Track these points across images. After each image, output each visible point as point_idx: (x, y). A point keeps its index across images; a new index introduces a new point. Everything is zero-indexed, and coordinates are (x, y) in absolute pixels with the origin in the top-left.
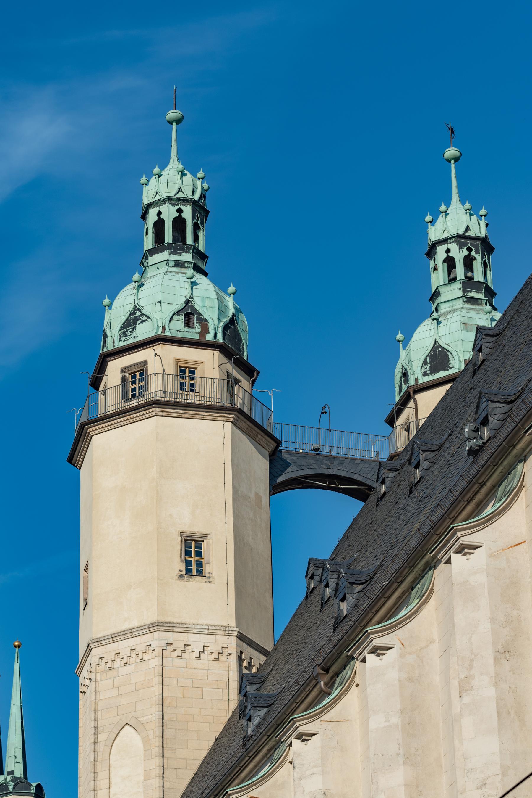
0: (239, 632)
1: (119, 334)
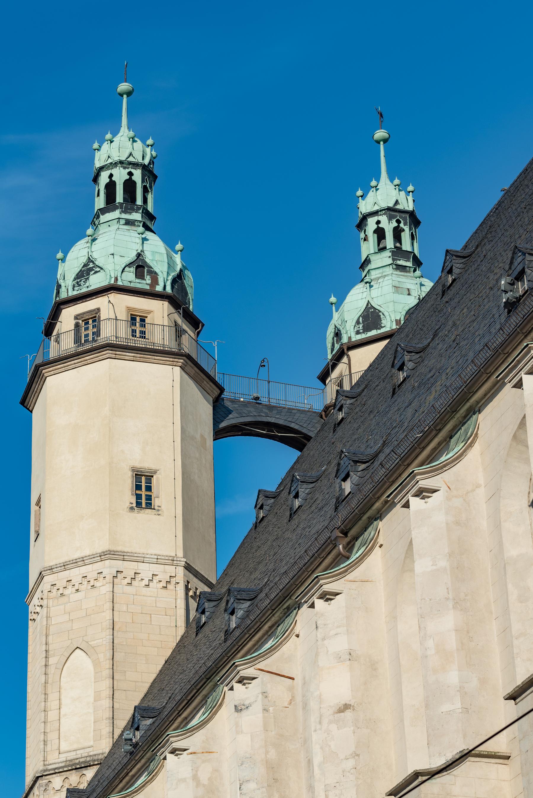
0: (186, 562)
1: (73, 284)
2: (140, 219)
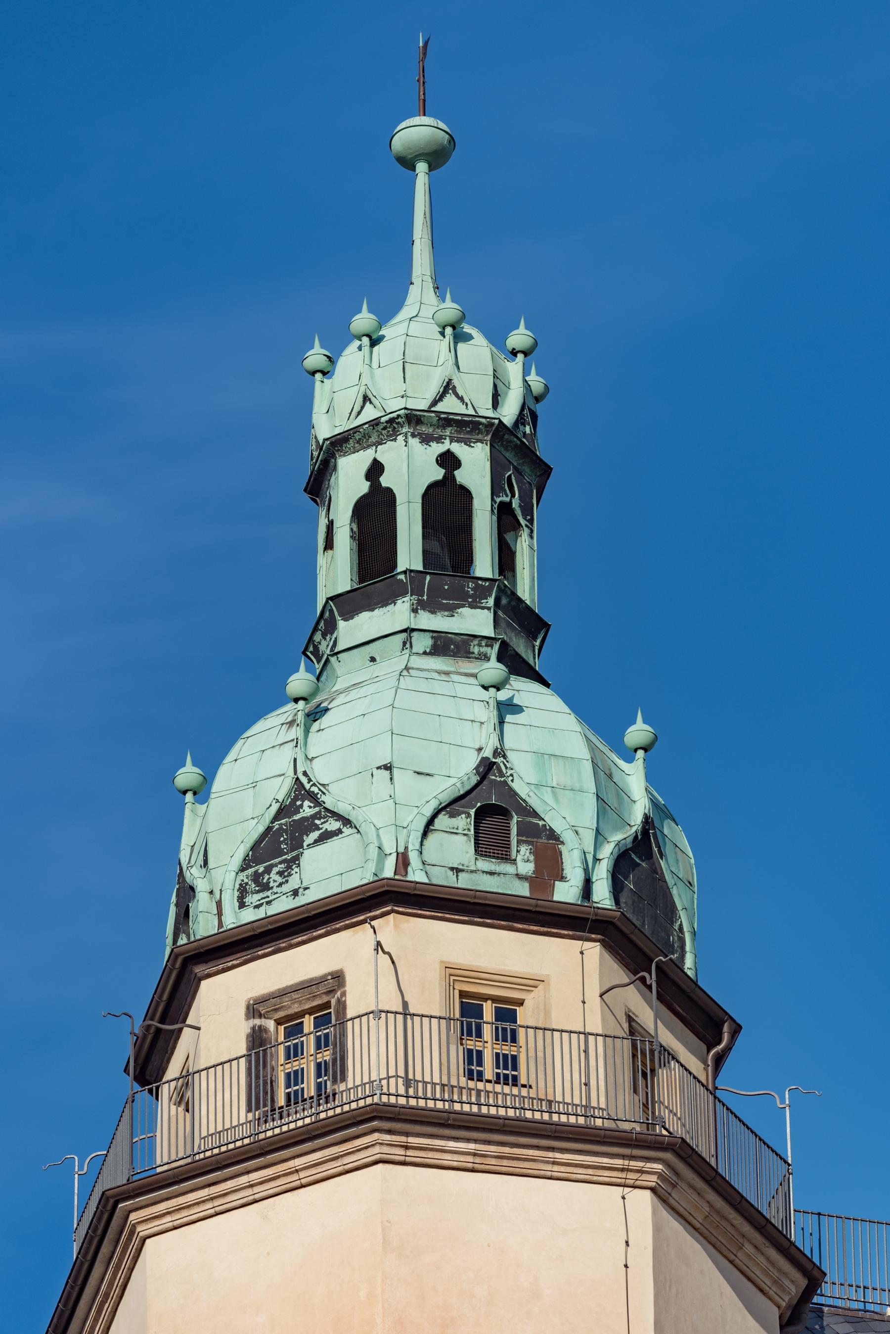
1: (238, 882)
2: (489, 631)
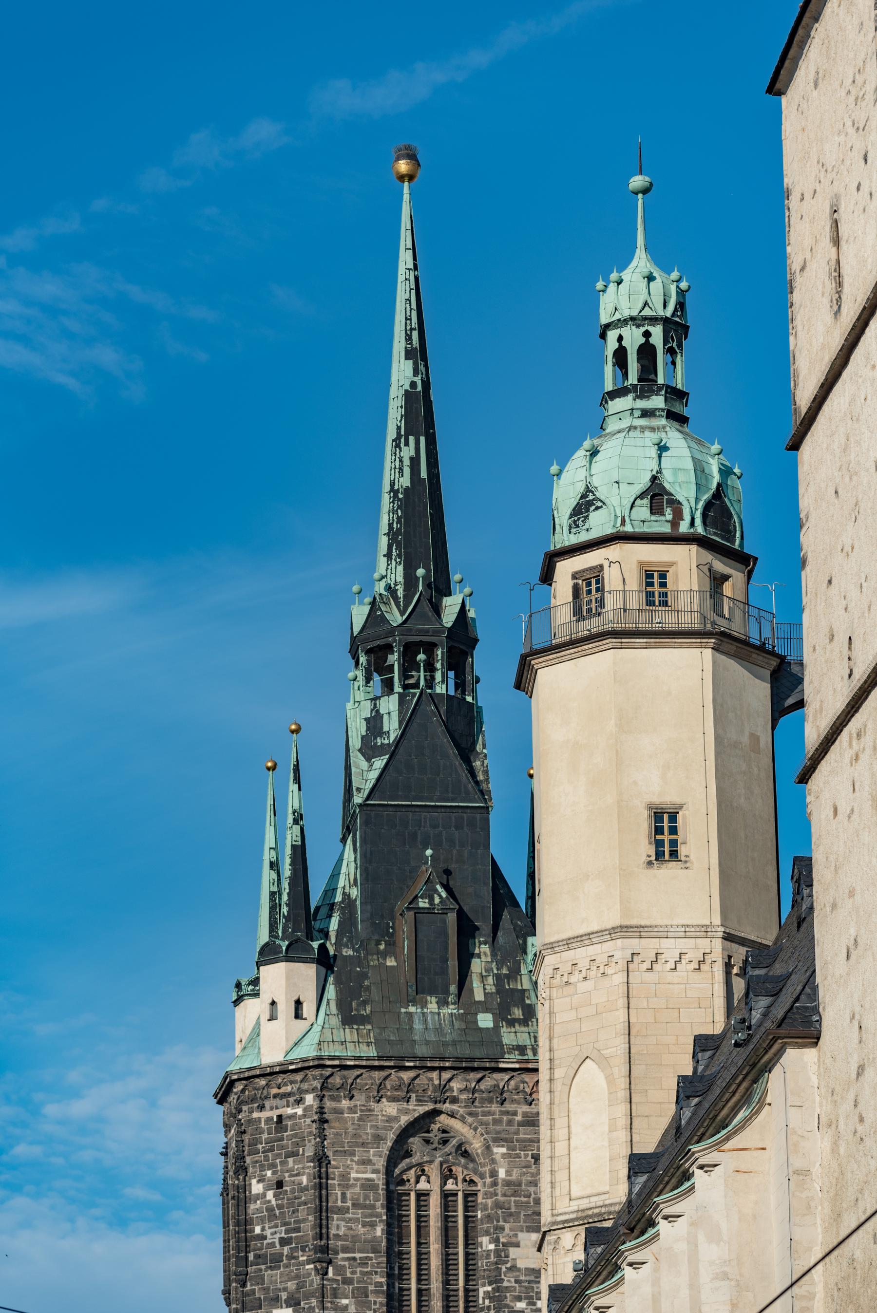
0: (724, 932)
2: (662, 405)
